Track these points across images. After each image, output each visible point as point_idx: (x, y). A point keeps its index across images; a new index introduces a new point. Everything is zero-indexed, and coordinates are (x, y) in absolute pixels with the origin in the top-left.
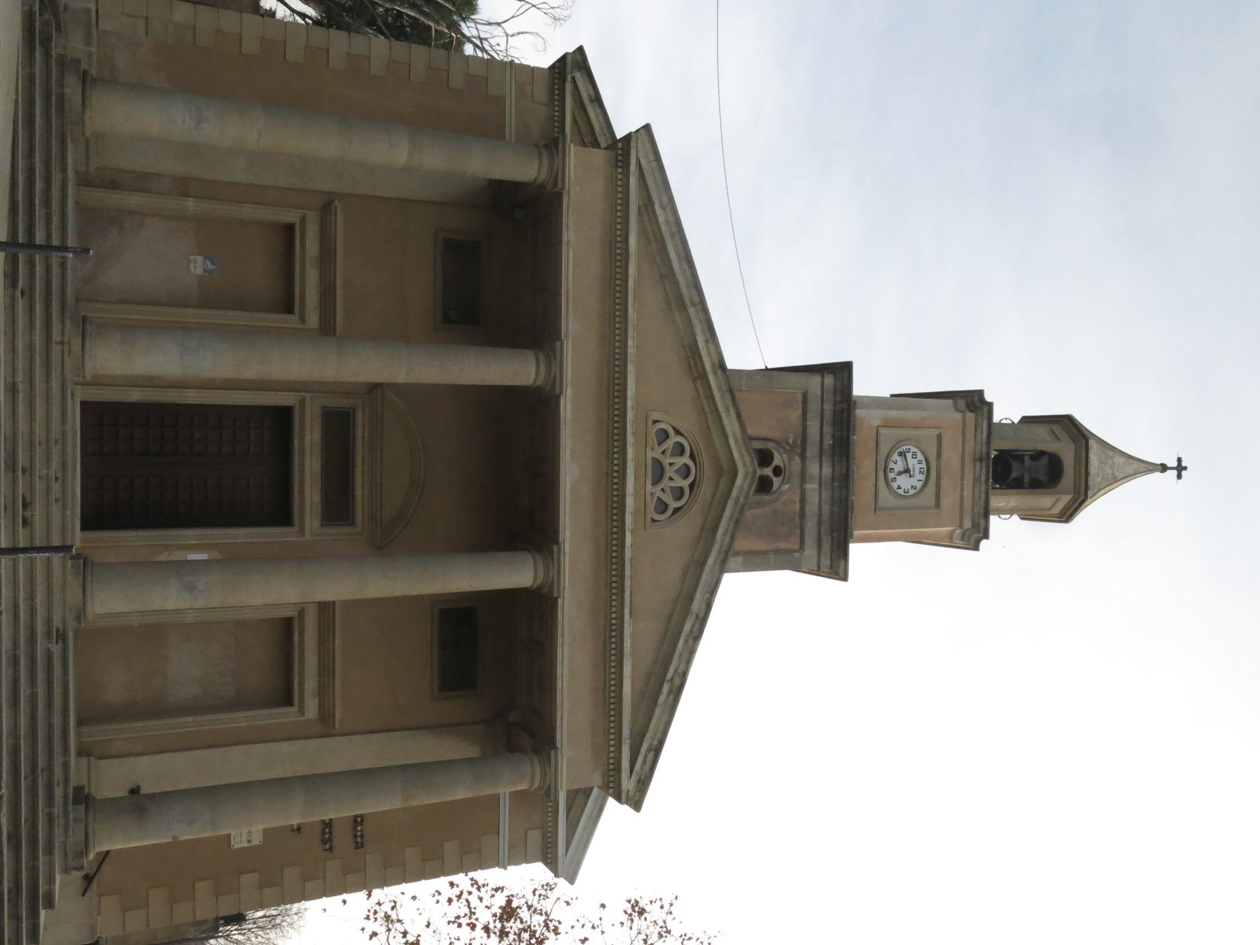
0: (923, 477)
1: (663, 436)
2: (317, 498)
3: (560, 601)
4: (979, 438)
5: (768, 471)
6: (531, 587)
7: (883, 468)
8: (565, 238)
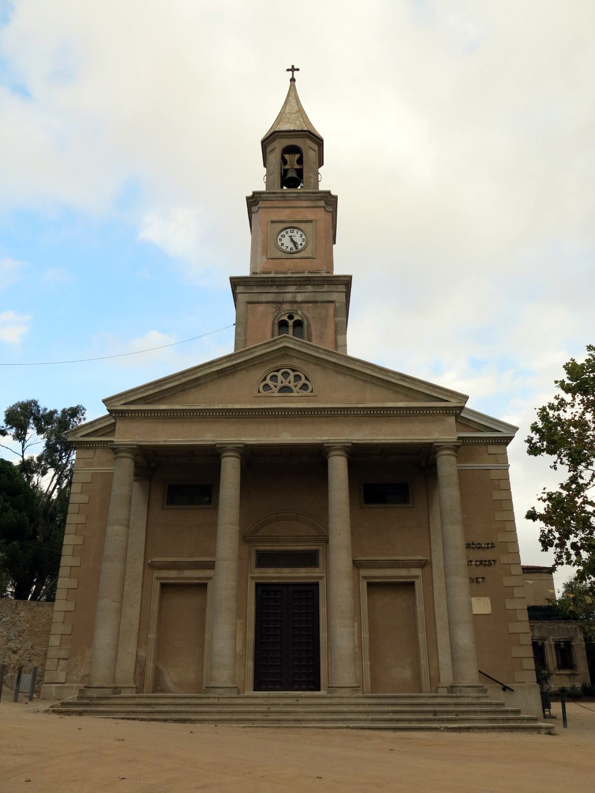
0: (295, 231)
1: (267, 387)
2: (304, 570)
3: (354, 442)
4: (273, 199)
5: (291, 322)
6: (347, 458)
8: (162, 443)
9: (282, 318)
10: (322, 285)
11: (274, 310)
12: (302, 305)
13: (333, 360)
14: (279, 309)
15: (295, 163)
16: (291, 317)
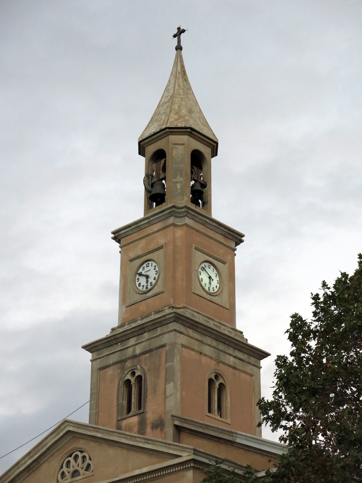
7: (145, 295)
9: (126, 378)
10: (156, 328)
11: (120, 371)
12: (141, 358)
13: (99, 435)
14: (123, 369)
15: (161, 171)
16: (133, 374)
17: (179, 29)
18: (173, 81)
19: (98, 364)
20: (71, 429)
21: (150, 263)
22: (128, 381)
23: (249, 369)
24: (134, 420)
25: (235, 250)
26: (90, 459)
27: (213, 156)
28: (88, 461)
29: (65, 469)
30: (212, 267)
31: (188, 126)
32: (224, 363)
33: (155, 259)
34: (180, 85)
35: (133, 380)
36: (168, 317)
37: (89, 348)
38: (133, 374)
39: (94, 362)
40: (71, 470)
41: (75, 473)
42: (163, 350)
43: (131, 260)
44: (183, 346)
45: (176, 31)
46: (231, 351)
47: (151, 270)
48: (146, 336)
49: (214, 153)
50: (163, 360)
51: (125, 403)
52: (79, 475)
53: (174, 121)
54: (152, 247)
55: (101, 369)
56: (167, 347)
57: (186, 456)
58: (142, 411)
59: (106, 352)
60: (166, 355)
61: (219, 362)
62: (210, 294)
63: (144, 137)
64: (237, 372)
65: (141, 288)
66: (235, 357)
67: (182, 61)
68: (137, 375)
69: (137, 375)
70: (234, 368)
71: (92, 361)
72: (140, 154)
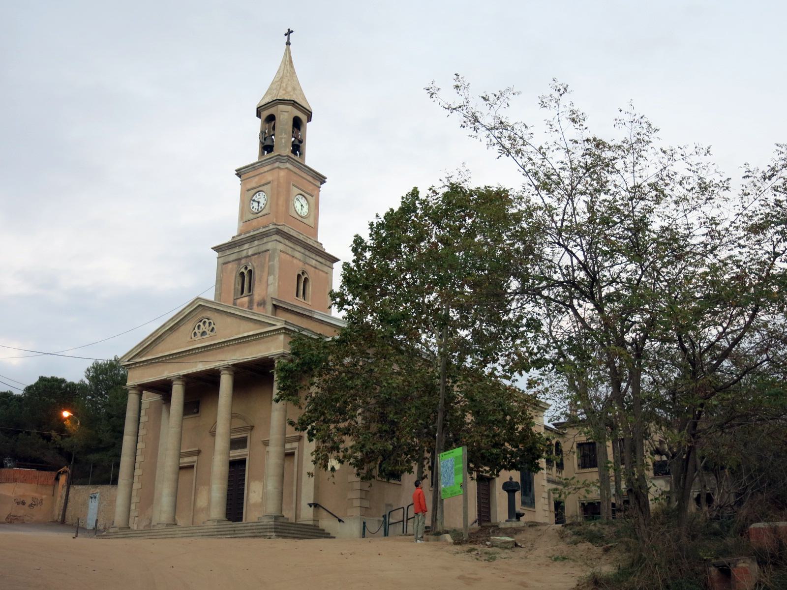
2: (239, 451)
8: (146, 382)
13: (221, 309)
14: (239, 264)
16: (246, 268)
17: (289, 30)
18: (283, 67)
19: (222, 260)
20: (202, 303)
21: (261, 193)
22: (242, 273)
23: (326, 269)
24: (246, 299)
25: (320, 188)
26: (214, 324)
27: (308, 122)
28: (212, 325)
29: (196, 330)
30: (303, 198)
31: (292, 99)
32: (308, 264)
33: (265, 190)
34: (287, 70)
35: (246, 272)
36: (272, 231)
37: (217, 249)
38: (246, 268)
39: (220, 259)
40: (201, 331)
41: (204, 333)
42: (268, 253)
43: (248, 190)
44: (281, 251)
45: (287, 31)
46: (313, 256)
47: (261, 198)
48: (256, 243)
49: (309, 119)
50: (267, 259)
51: (240, 288)
52: (206, 334)
53: (282, 95)
54: (263, 182)
55: (224, 264)
56: (270, 252)
57: (279, 325)
58: (251, 293)
59: (228, 252)
60: (269, 257)
61: (305, 263)
62: (301, 217)
63: (261, 105)
64: (317, 270)
65: (254, 210)
66: (316, 260)
67: (290, 53)
68: (248, 269)
69: (248, 269)
70: (315, 268)
71: (218, 258)
72: (257, 116)
